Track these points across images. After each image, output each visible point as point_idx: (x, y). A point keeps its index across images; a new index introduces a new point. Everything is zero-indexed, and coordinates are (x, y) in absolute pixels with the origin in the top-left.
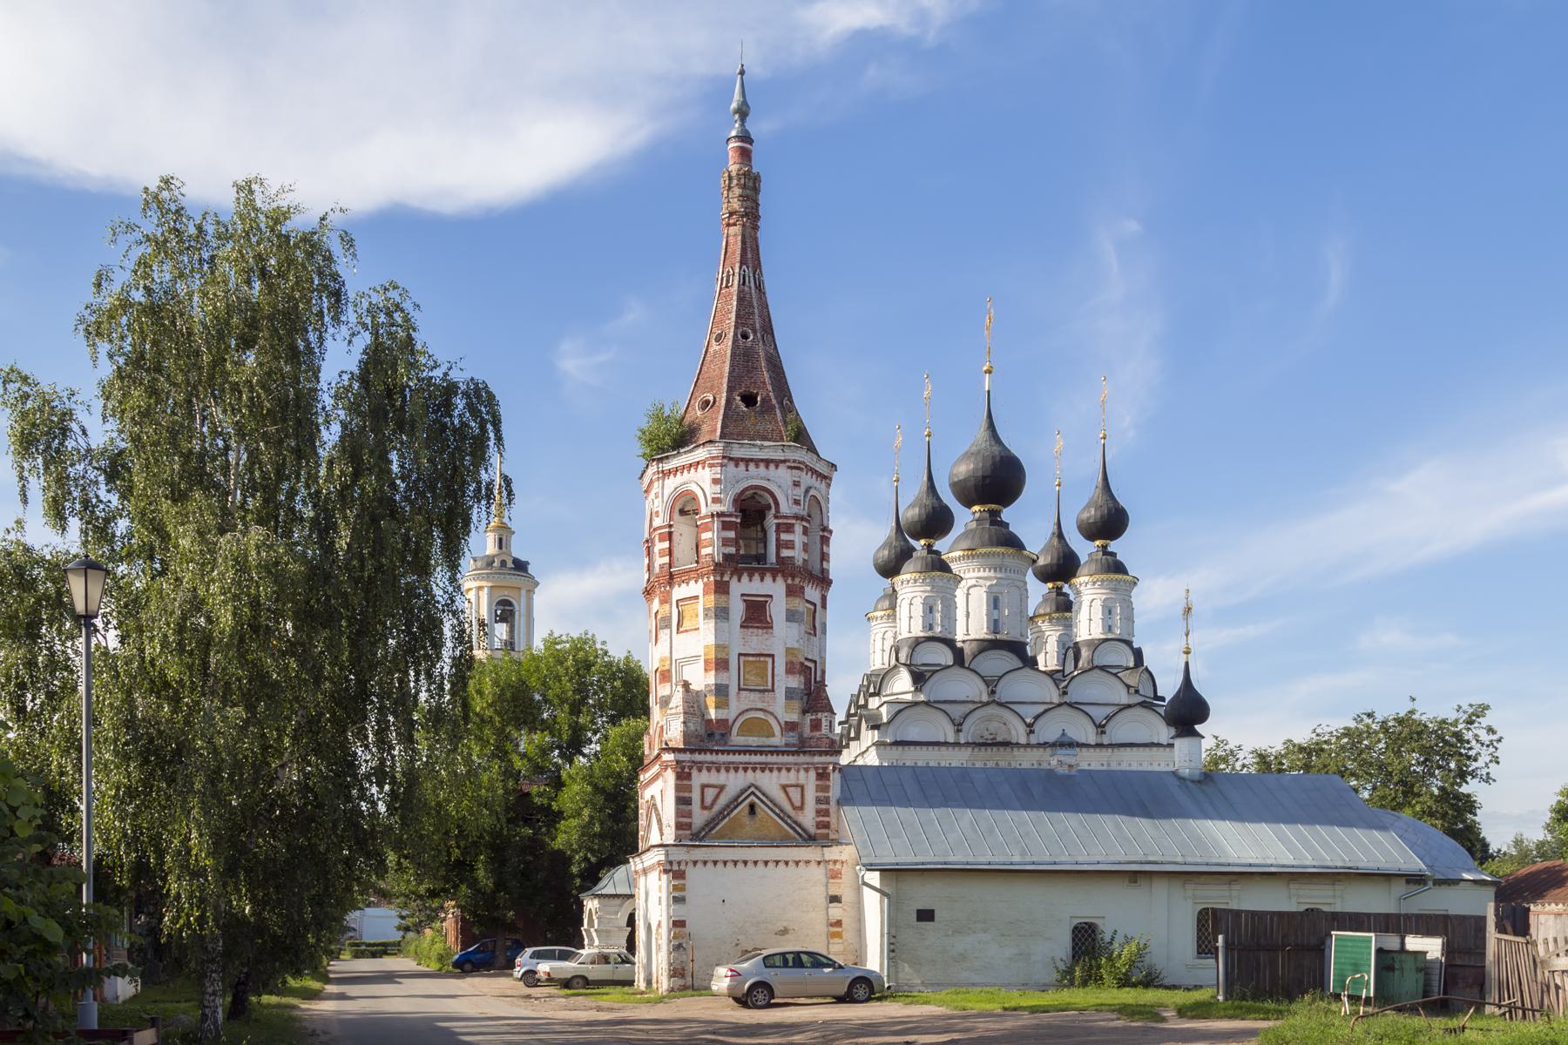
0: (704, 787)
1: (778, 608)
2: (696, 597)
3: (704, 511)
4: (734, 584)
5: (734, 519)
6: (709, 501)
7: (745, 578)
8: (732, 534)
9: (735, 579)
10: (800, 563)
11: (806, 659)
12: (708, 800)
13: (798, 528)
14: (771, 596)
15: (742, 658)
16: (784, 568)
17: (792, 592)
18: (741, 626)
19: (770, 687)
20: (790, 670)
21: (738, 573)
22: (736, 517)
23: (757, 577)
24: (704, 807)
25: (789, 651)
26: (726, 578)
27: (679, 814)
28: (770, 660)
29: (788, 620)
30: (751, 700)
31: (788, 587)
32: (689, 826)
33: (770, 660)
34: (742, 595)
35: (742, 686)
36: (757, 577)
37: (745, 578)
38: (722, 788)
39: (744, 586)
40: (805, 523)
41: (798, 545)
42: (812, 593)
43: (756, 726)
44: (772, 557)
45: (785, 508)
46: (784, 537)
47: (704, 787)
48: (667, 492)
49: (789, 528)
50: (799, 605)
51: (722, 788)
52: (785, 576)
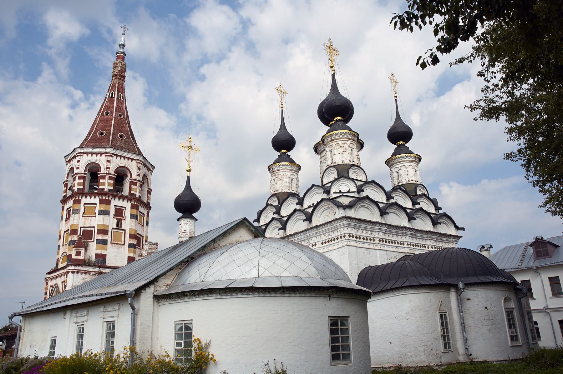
1: (128, 212)
2: (96, 204)
3: (103, 170)
5: (114, 176)
6: (106, 168)
8: (112, 182)
9: (113, 199)
10: (137, 196)
11: (138, 234)
13: (138, 184)
14: (125, 208)
15: (113, 230)
16: (131, 197)
17: (133, 207)
18: (113, 218)
19: (123, 243)
20: (131, 236)
21: (114, 197)
22: (115, 175)
23: (121, 200)
26: (110, 199)
28: (123, 232)
29: (130, 218)
31: (132, 204)
33: (123, 232)
34: (115, 206)
35: (112, 242)
36: (121, 200)
37: (117, 199)
39: (116, 202)
40: (140, 183)
41: (138, 190)
42: (142, 209)
44: (126, 192)
45: (134, 176)
46: (133, 187)
48: (84, 162)
49: (135, 184)
50: (135, 212)
52: (131, 202)
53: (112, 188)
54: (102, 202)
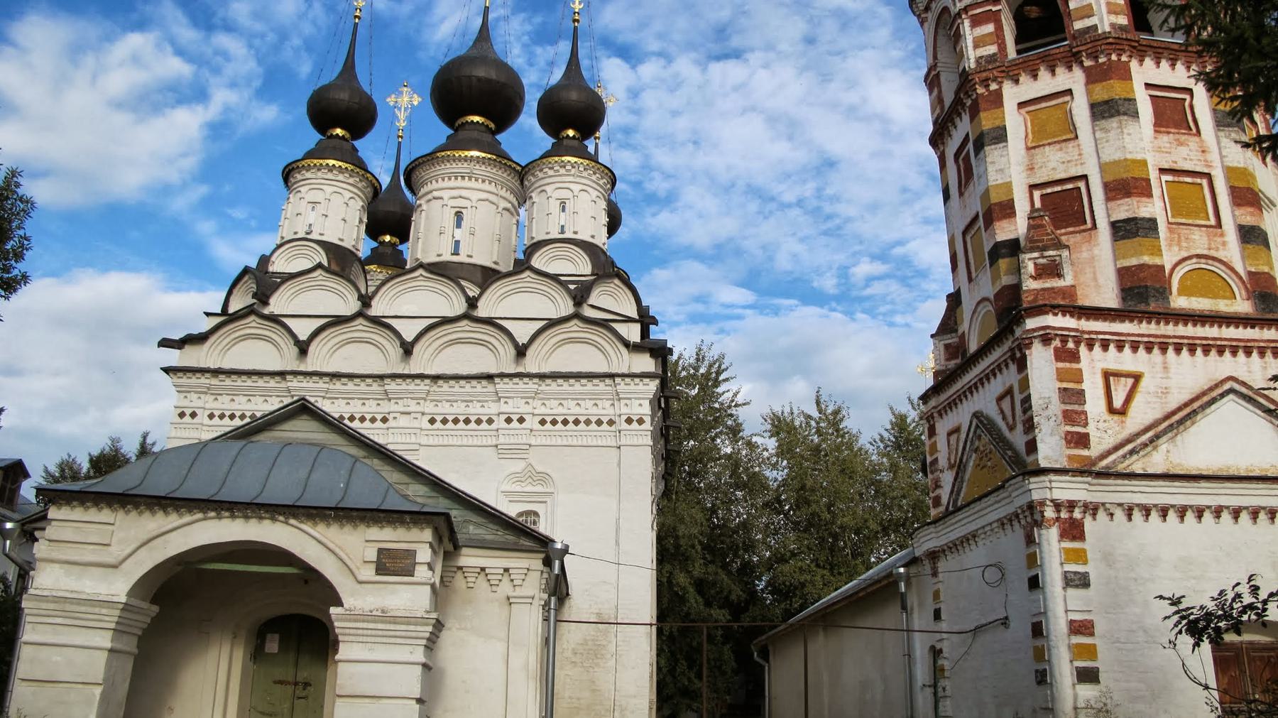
0: (1107, 375)
4: (1134, 64)
7: (1148, 62)
12: (1118, 402)
21: (1140, 52)
24: (1111, 410)
25: (1230, 172)
27: (1069, 417)
30: (1199, 241)
32: (1082, 440)
34: (1148, 86)
37: (1148, 62)
38: (1137, 378)
43: (1201, 281)
47: (1107, 375)
51: (1137, 378)
53: (1123, 20)
54: (1092, 78)
